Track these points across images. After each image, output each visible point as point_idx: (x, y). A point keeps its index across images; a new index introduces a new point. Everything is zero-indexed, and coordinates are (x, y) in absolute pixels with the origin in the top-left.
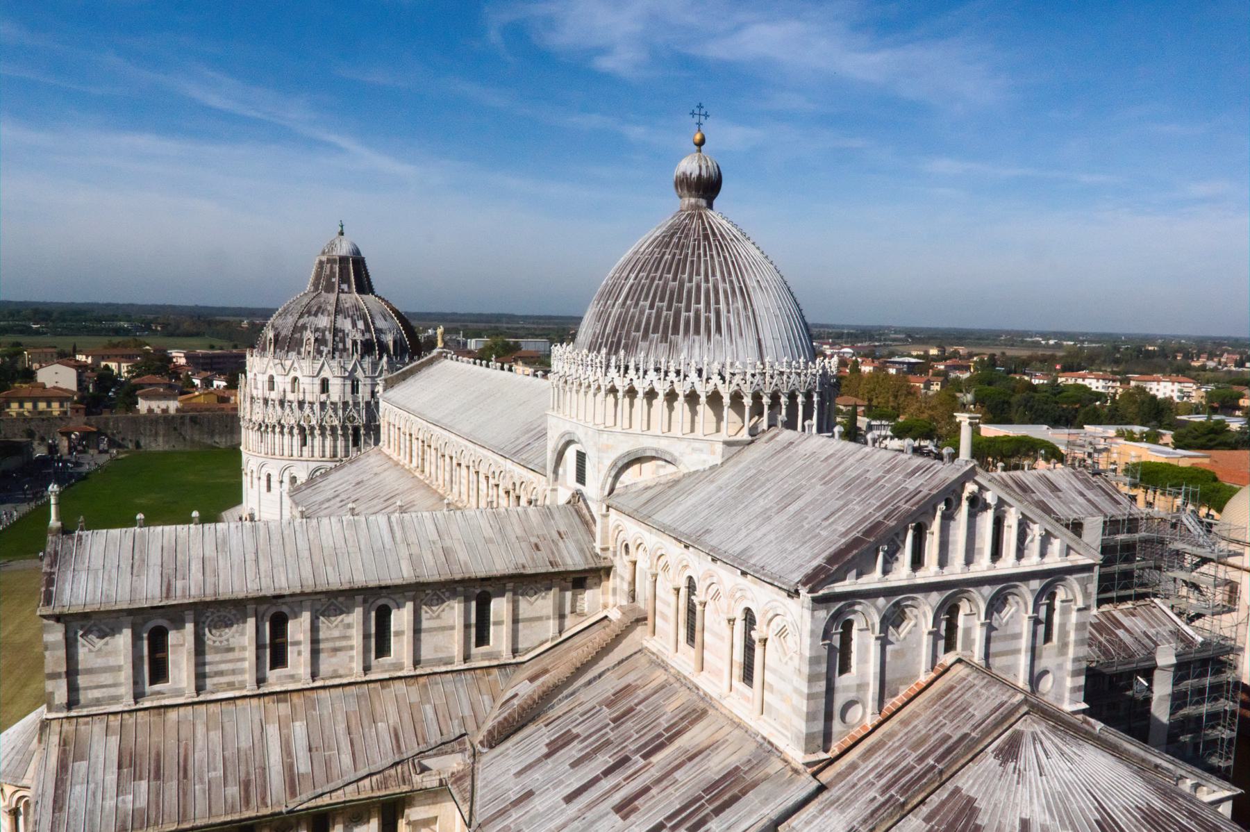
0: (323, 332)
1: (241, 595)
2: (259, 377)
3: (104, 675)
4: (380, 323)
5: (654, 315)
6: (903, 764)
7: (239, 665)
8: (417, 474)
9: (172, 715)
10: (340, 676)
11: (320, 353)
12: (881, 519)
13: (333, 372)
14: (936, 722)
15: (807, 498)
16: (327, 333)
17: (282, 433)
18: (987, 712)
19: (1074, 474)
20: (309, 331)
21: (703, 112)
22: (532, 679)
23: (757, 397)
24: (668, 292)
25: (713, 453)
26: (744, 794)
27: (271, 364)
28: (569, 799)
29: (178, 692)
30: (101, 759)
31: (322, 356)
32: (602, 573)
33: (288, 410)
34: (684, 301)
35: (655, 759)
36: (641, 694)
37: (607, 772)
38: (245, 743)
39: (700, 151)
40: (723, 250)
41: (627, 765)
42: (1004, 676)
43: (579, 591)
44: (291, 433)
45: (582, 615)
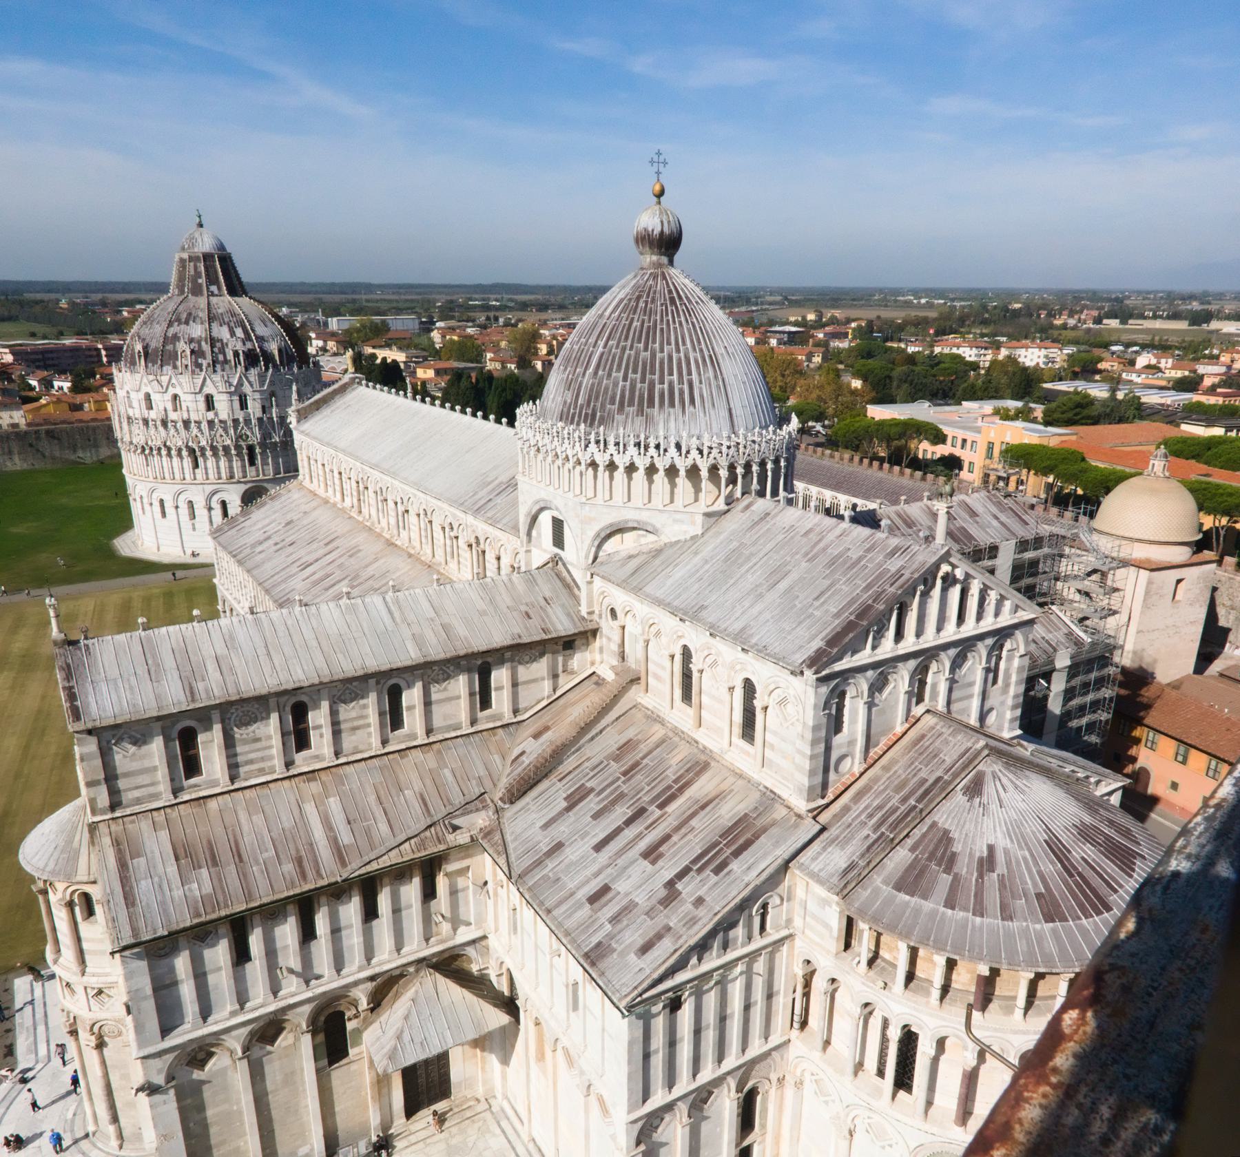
0: (199, 342)
1: (264, 691)
2: (133, 395)
3: (141, 776)
4: (261, 330)
5: (628, 387)
6: (889, 805)
7: (267, 752)
8: (354, 514)
10: (361, 752)
13: (216, 386)
14: (913, 767)
15: (793, 576)
16: (203, 343)
17: (169, 455)
18: (955, 757)
20: (182, 342)
22: (536, 736)
23: (732, 468)
24: (640, 363)
25: (693, 523)
26: (757, 838)
27: (145, 380)
28: (598, 847)
29: (215, 783)
30: (157, 854)
31: (201, 370)
32: (589, 634)
33: (172, 431)
34: (657, 372)
35: (670, 808)
36: (644, 748)
37: (629, 822)
38: (287, 822)
39: (659, 203)
40: (690, 315)
41: (645, 815)
42: (959, 718)
43: (568, 652)
44: (179, 455)
45: (572, 673)
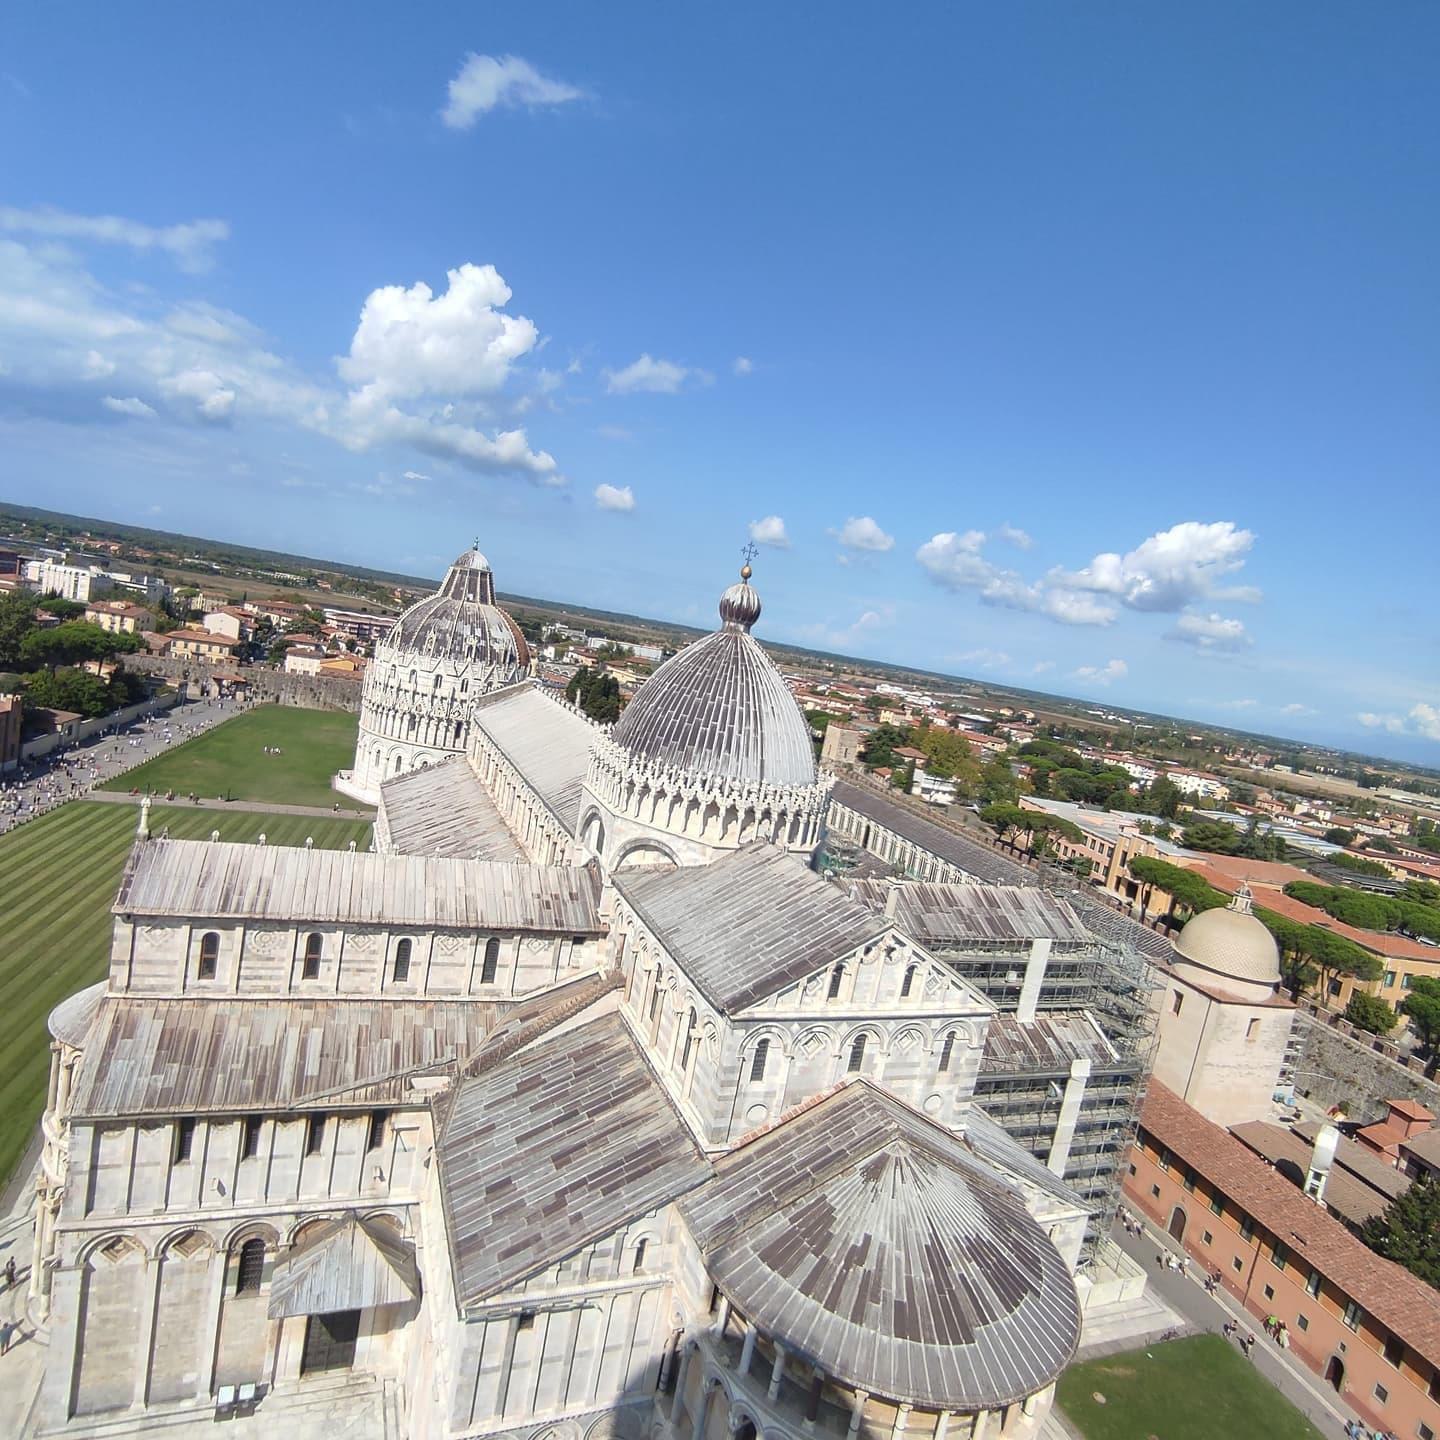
7: (276, 972)
8: (489, 791)
9: (213, 1008)
11: (438, 652)
12: (807, 958)
19: (1039, 894)
21: (753, 549)
22: (523, 1020)
23: (750, 812)
25: (704, 854)
28: (519, 1140)
29: (223, 990)
30: (145, 1039)
35: (599, 1119)
37: (556, 1122)
38: (268, 1040)
42: (898, 1097)
